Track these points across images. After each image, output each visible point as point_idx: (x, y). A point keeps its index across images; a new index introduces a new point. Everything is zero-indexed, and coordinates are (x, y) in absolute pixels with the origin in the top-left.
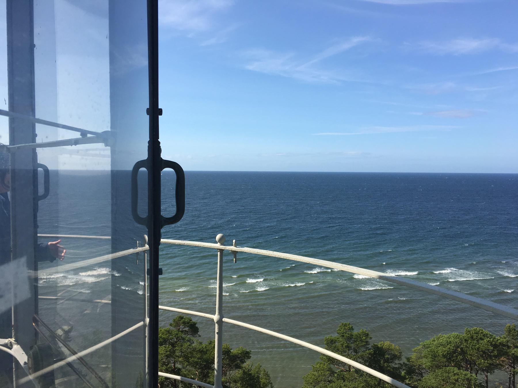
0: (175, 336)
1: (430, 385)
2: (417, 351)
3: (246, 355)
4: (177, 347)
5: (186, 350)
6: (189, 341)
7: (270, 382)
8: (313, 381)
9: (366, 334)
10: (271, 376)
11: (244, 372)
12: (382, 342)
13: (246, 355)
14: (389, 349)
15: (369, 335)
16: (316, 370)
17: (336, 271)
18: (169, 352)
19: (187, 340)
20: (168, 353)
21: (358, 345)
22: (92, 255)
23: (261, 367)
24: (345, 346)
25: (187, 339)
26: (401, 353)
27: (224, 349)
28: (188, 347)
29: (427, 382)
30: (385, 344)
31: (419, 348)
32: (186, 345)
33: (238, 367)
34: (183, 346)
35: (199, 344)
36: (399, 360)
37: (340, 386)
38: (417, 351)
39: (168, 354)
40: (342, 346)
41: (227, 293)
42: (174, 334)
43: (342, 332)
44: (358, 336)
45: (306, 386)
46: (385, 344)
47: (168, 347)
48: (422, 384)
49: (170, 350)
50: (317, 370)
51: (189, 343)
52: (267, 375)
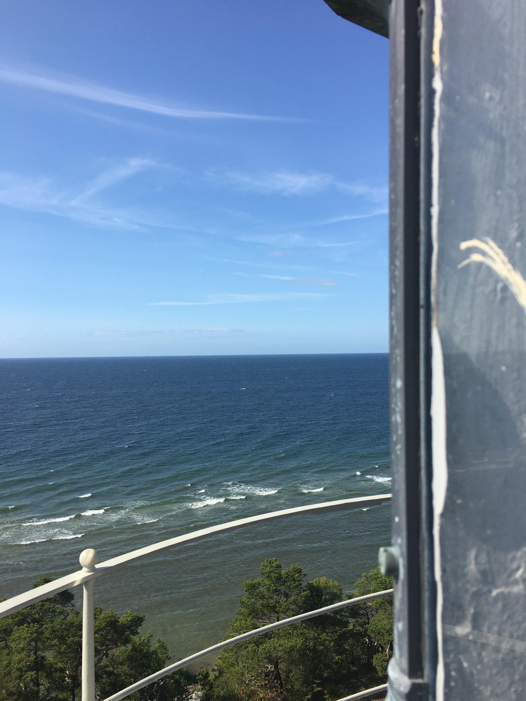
0: (41, 609)
1: (382, 627)
2: (360, 585)
3: (138, 621)
4: (44, 624)
5: (60, 627)
6: (61, 613)
7: (169, 657)
8: (234, 647)
9: (298, 569)
10: (169, 647)
11: (134, 649)
12: (317, 579)
13: (138, 621)
14: (326, 588)
15: (302, 571)
16: (236, 630)
17: (465, 566)
18: (35, 633)
19: (59, 612)
20: (35, 635)
21: (289, 587)
22: (105, 530)
23: (152, 636)
24: (272, 590)
25: (58, 611)
26: (341, 589)
27: (110, 618)
28: (63, 623)
29: (377, 624)
30: (321, 581)
31: (362, 580)
32: (59, 619)
33: (126, 641)
34: (54, 622)
35: (76, 615)
36: (340, 600)
37: (274, 646)
38: (360, 585)
39: (35, 637)
40: (269, 590)
41: (498, 595)
42: (38, 606)
43: (268, 571)
44: (289, 574)
45: (224, 655)
46: (321, 581)
47: (33, 626)
48: (371, 628)
49: (36, 630)
50: (237, 630)
51: (62, 617)
52: (164, 647)
